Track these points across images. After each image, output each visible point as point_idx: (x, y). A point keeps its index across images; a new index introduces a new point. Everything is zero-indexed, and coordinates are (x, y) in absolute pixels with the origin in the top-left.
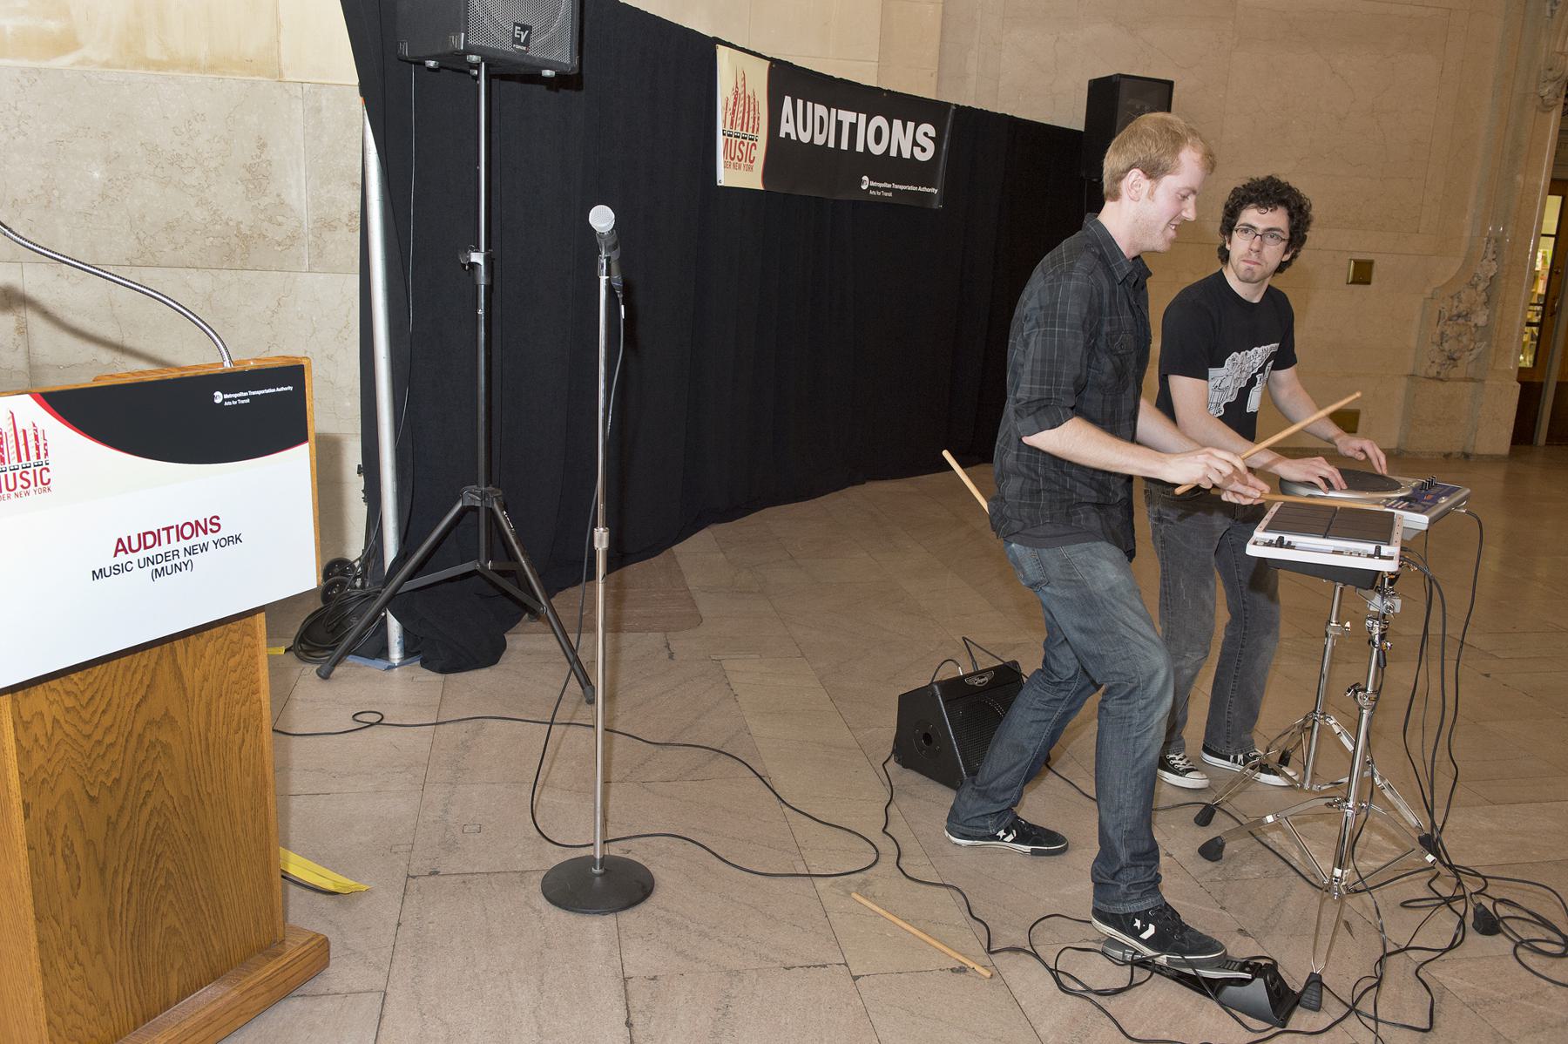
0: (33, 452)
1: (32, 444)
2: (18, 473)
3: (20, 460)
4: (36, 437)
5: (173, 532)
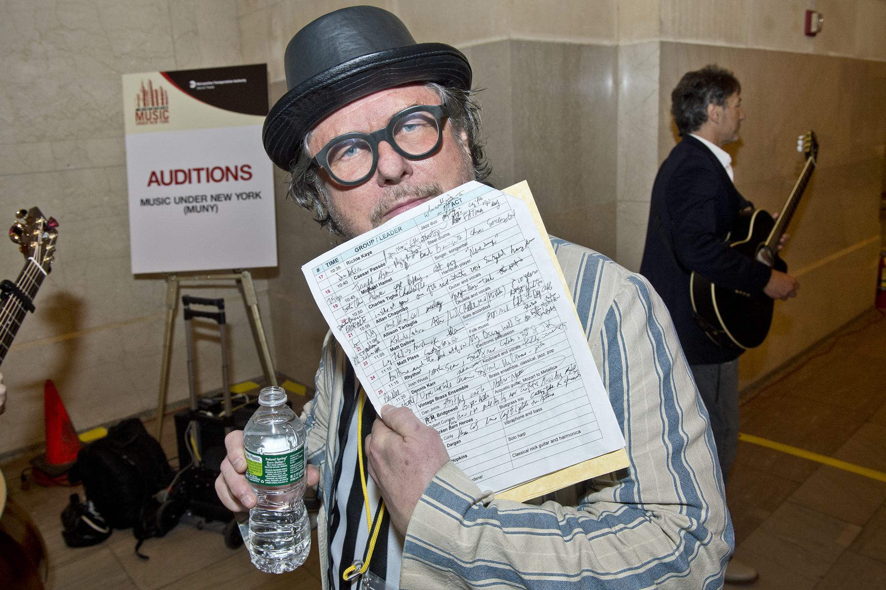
0: (160, 101)
1: (160, 97)
3: (153, 104)
5: (203, 174)
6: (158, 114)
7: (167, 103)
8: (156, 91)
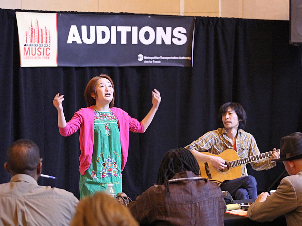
0: (44, 40)
1: (44, 36)
2: (37, 48)
3: (38, 42)
6: (42, 51)
7: (50, 42)
8: (42, 30)
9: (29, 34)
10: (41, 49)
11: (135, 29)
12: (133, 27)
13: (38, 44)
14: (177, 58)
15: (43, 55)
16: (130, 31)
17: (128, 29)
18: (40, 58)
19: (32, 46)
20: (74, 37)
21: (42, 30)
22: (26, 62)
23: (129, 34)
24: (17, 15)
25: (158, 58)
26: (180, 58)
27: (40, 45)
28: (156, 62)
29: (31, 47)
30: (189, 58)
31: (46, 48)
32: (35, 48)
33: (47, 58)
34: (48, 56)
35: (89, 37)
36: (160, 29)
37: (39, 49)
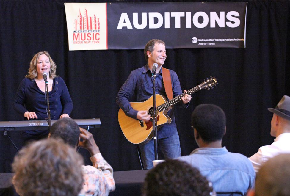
0: (93, 26)
1: (93, 23)
2: (86, 33)
3: (88, 28)
4: (95, 21)
6: (91, 36)
7: (99, 28)
8: (91, 18)
9: (78, 21)
10: (90, 34)
11: (189, 14)
12: (187, 13)
13: (88, 30)
14: (232, 40)
15: (93, 40)
16: (184, 16)
17: (182, 14)
18: (89, 42)
19: (82, 32)
20: (125, 23)
21: (91, 18)
22: (73, 46)
23: (183, 20)
24: (65, 5)
25: (212, 40)
26: (234, 40)
27: (89, 31)
28: (210, 44)
29: (80, 33)
30: (242, 40)
31: (95, 33)
32: (85, 34)
33: (97, 42)
34: (98, 41)
35: (140, 22)
36: (213, 14)
37: (89, 35)
